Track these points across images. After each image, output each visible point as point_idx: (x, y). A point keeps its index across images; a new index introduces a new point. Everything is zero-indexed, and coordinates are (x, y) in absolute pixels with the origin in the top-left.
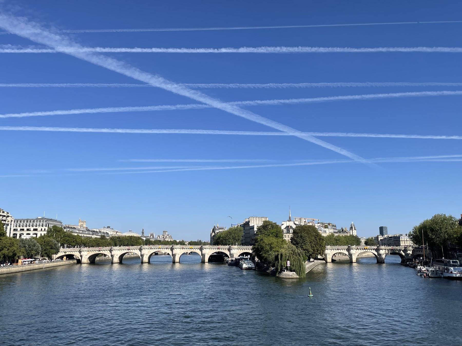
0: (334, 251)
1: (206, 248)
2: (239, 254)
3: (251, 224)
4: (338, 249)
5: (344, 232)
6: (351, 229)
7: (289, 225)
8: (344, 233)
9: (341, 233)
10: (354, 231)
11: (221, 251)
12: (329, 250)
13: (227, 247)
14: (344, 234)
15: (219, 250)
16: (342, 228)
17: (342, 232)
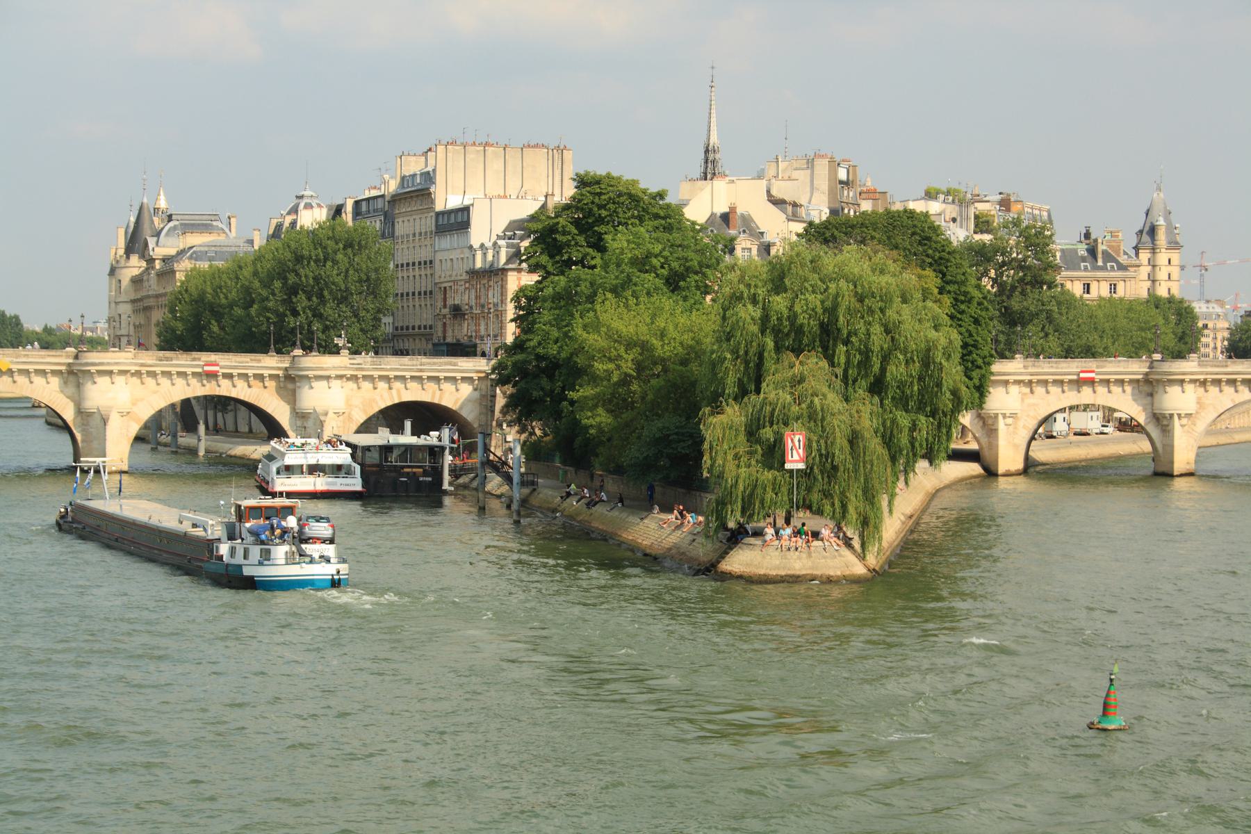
0: (1050, 397)
1: (115, 368)
2: (361, 418)
3: (447, 198)
4: (1079, 383)
5: (1100, 263)
6: (1146, 238)
7: (733, 210)
8: (1104, 268)
9: (1079, 269)
10: (1162, 258)
11: (224, 389)
12: (1014, 389)
13: (271, 363)
14: (1100, 274)
15: (210, 389)
16: (1087, 235)
17: (1084, 259)
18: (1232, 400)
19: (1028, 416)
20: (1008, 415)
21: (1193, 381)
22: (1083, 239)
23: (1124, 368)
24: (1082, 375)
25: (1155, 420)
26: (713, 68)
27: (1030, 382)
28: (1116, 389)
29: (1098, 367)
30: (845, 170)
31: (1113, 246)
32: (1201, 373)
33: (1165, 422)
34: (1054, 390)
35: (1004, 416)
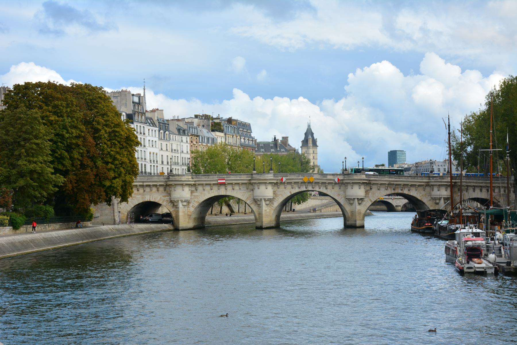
5: (278, 149)
16: (275, 138)
17: (272, 148)
18: (290, 192)
19: (194, 201)
20: (183, 201)
21: (270, 183)
22: (273, 140)
23: (240, 178)
24: (219, 181)
25: (254, 202)
26: (144, 82)
27: (195, 185)
28: (237, 187)
29: (227, 178)
30: (138, 98)
31: (284, 143)
32: (275, 180)
33: (259, 203)
34: (208, 188)
35: (182, 202)
